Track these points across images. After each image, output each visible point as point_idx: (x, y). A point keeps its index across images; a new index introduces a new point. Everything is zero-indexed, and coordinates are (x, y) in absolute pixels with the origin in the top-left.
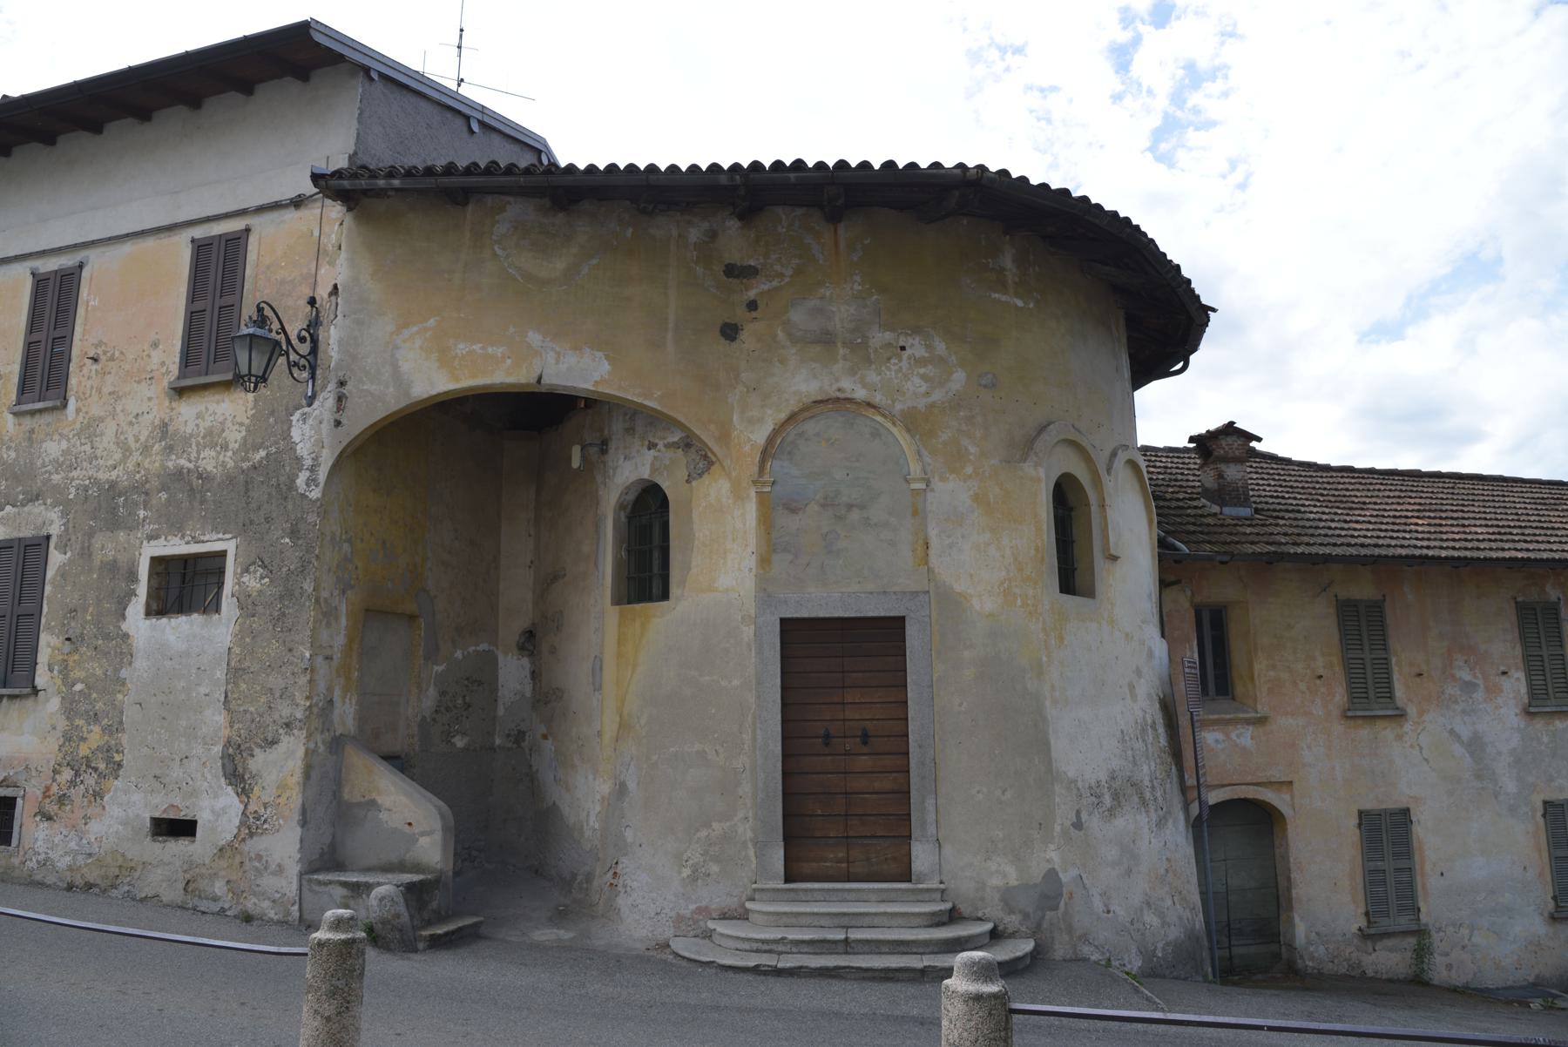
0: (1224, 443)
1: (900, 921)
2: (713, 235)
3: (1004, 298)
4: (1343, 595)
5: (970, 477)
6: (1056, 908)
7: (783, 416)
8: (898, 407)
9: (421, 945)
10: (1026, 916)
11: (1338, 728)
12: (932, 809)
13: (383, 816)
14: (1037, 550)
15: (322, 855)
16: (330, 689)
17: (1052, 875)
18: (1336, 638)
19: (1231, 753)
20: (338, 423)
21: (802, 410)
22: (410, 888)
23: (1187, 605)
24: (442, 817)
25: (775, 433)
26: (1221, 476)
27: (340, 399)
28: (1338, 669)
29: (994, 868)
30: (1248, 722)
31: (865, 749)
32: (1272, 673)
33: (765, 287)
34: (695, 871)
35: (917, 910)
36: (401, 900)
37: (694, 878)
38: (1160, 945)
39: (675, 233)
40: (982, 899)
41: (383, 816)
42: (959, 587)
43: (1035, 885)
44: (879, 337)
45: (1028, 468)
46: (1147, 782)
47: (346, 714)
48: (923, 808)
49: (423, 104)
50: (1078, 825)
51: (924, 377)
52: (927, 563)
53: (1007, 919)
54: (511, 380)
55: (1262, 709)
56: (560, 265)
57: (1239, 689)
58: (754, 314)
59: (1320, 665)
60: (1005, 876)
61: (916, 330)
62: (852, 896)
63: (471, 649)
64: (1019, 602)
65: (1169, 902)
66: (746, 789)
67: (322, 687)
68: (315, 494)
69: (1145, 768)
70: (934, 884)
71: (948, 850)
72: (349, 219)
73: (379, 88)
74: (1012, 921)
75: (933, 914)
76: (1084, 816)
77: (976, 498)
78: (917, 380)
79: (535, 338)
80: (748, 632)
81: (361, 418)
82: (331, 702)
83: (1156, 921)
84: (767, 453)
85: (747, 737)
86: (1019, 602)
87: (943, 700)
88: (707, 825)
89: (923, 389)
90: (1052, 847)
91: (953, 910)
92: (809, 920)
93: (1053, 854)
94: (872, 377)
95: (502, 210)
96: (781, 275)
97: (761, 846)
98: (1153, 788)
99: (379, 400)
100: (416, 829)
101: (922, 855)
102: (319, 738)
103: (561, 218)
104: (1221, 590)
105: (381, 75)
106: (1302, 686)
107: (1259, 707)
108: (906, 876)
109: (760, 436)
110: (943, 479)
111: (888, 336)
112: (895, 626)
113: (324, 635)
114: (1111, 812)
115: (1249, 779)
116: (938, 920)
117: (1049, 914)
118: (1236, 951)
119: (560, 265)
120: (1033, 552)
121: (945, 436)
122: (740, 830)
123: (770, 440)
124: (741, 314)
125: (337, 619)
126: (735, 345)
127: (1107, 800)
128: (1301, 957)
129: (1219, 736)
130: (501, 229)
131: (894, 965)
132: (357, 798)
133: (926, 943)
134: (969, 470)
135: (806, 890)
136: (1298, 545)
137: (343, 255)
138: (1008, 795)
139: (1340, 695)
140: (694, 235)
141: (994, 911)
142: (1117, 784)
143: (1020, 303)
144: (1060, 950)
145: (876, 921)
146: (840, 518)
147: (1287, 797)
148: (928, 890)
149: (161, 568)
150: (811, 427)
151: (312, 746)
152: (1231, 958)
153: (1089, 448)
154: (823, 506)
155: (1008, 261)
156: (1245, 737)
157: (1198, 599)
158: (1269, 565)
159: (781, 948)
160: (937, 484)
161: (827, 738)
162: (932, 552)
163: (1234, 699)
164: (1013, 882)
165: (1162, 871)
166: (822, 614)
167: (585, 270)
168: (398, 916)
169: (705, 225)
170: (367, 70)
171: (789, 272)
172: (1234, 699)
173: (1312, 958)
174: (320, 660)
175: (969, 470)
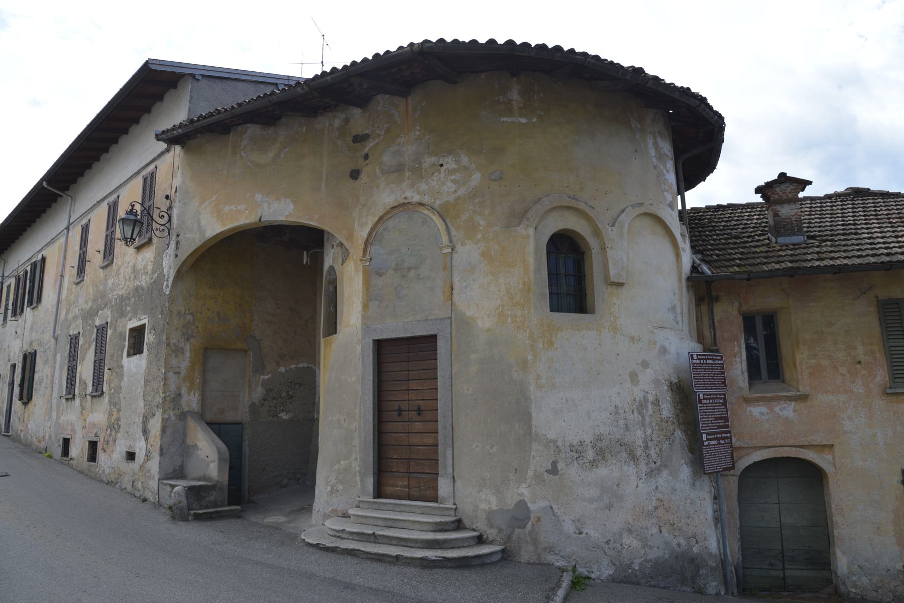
0: (778, 190)
1: (418, 526)
2: (347, 121)
3: (510, 120)
4: (884, 295)
5: (479, 240)
6: (524, 527)
7: (376, 219)
8: (438, 202)
9: (190, 518)
10: (500, 531)
11: (879, 403)
12: (450, 457)
13: (199, 452)
14: (524, 284)
15: (174, 471)
16: (179, 388)
17: (522, 504)
18: (877, 330)
19: (766, 424)
20: (176, 256)
21: (385, 214)
22: (191, 489)
23: (735, 313)
24: (219, 453)
25: (372, 229)
26: (776, 215)
27: (177, 243)
28: (880, 355)
29: (483, 497)
30: (790, 399)
31: (419, 419)
32: (813, 361)
33: (372, 145)
34: (332, 488)
35: (425, 520)
36: (184, 494)
37: (332, 492)
38: (637, 561)
39: (327, 124)
40: (476, 517)
41: (199, 452)
42: (469, 314)
43: (509, 510)
44: (428, 161)
45: (521, 230)
46: (640, 442)
47: (191, 401)
48: (445, 456)
49: (240, 84)
50: (554, 470)
51: (454, 182)
52: (451, 299)
53: (489, 532)
54: (248, 221)
55: (804, 389)
56: (271, 155)
57: (787, 374)
58: (367, 162)
59: (860, 352)
60: (489, 503)
61: (450, 152)
62: (407, 509)
63: (293, 367)
64: (510, 320)
65: (655, 530)
66: (356, 442)
67: (173, 387)
68: (167, 293)
69: (639, 433)
70: (450, 505)
71: (459, 483)
72: (182, 153)
73: (205, 82)
74: (491, 533)
75: (437, 523)
76: (560, 466)
77: (483, 254)
78: (449, 184)
79: (258, 197)
80: (359, 349)
81: (187, 249)
82: (180, 395)
83: (635, 543)
84: (367, 243)
85: (357, 411)
86: (510, 320)
87: (460, 385)
88: (339, 462)
89: (452, 190)
90: (524, 485)
91: (459, 521)
92: (370, 521)
93: (524, 491)
94: (423, 187)
95: (245, 132)
96: (379, 135)
97: (363, 476)
98: (647, 447)
99: (193, 241)
100: (210, 459)
101: (444, 487)
102: (171, 413)
103: (271, 130)
104: (764, 300)
105: (203, 76)
106: (843, 370)
107: (801, 388)
108: (435, 499)
109: (365, 234)
110: (463, 244)
111: (433, 159)
112: (432, 339)
113: (174, 362)
114: (593, 464)
115: (791, 442)
116: (441, 528)
117: (517, 531)
118: (789, 573)
119: (271, 155)
120: (521, 286)
121: (464, 217)
122: (353, 465)
123: (370, 234)
124: (361, 162)
125: (183, 353)
126: (357, 182)
127: (590, 455)
128: (844, 583)
129: (764, 409)
130: (245, 142)
131: (381, 552)
132: (191, 444)
133: (416, 541)
134: (479, 236)
135: (410, 506)
136: (822, 259)
137: (180, 171)
138: (495, 449)
139: (881, 376)
140: (337, 123)
141: (482, 526)
142: (603, 444)
143: (524, 121)
144: (526, 554)
145: (406, 525)
146: (404, 276)
147: (830, 457)
148: (447, 509)
149: (135, 334)
150: (391, 223)
151: (166, 416)
152: (784, 578)
153: (587, 209)
154: (395, 270)
155: (515, 95)
156: (788, 410)
157: (745, 308)
158: (801, 278)
159: (344, 536)
160: (459, 248)
161: (400, 411)
162: (455, 292)
163: (784, 382)
164: (494, 508)
165: (650, 508)
166: (394, 336)
167: (282, 155)
168: (180, 502)
169: (344, 116)
170: (193, 76)
171: (383, 133)
172: (784, 382)
173: (855, 586)
174: (171, 374)
175: (479, 236)
